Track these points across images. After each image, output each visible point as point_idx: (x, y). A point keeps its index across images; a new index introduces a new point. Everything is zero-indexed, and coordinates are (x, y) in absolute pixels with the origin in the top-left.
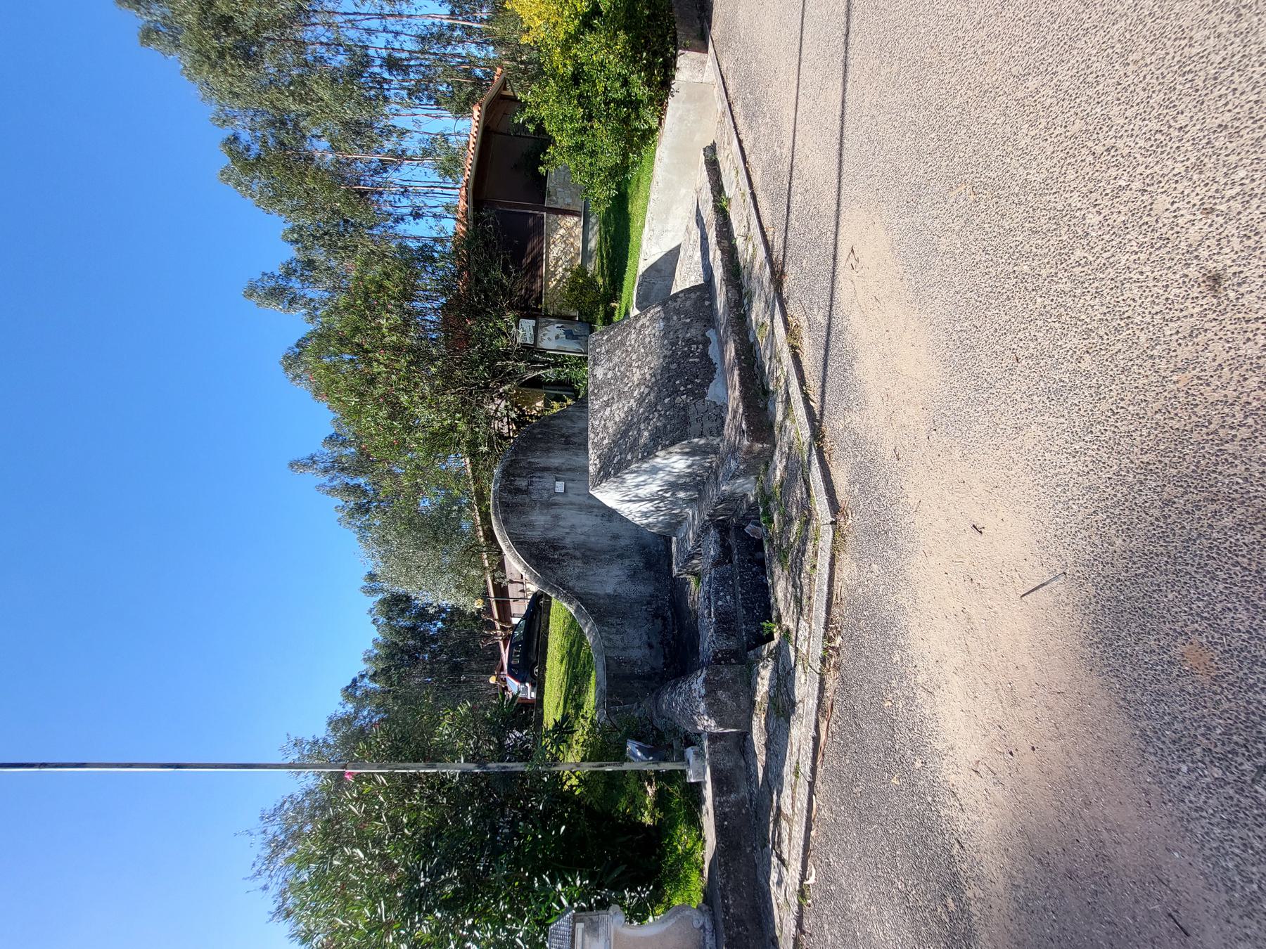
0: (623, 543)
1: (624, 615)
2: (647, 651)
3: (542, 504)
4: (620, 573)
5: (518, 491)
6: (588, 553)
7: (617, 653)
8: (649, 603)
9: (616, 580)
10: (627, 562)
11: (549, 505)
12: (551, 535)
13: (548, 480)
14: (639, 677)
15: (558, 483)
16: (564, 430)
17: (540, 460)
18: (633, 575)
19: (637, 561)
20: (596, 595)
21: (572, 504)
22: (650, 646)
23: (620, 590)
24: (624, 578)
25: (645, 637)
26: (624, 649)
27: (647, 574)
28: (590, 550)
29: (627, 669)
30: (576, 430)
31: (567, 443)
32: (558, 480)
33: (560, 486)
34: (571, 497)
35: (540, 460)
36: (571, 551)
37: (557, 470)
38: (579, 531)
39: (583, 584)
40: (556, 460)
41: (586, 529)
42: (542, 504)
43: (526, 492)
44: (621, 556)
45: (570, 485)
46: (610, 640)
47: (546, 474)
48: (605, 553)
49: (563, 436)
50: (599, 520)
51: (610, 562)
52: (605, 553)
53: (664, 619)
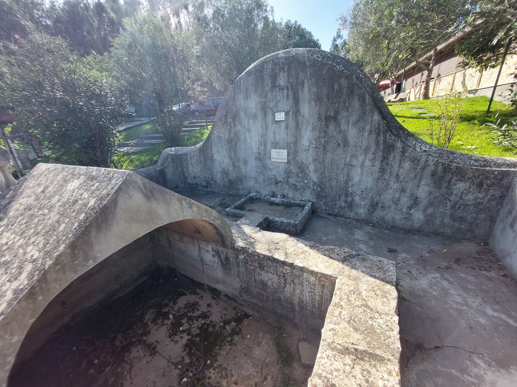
0: (242, 167)
1: (205, 165)
2: (193, 176)
3: (265, 102)
4: (225, 163)
5: (274, 78)
6: (233, 143)
7: (189, 159)
8: (212, 179)
9: (221, 161)
10: (231, 168)
11: (264, 109)
12: (242, 114)
13: (286, 104)
14: (183, 170)
15: (283, 114)
16: (344, 114)
17: (306, 94)
18: (225, 172)
19: (233, 175)
20: (212, 148)
21: (266, 128)
22: (195, 177)
23: (216, 163)
24: (223, 166)
25: (198, 175)
26: (191, 163)
27: (226, 180)
28: (236, 144)
29: (184, 165)
30: (344, 127)
31: (328, 119)
32: (287, 114)
33: (280, 116)
34: (272, 128)
35: (306, 94)
36: (233, 131)
37: (297, 112)
38: (247, 136)
39: (216, 140)
40: (308, 110)
41: (249, 140)
42: (265, 102)
43: (274, 86)
44: (234, 165)
45: (283, 125)
46: (194, 155)
47: (291, 101)
48: (235, 154)
49: (337, 113)
50: (255, 150)
51: (230, 158)
52: (235, 154)
53: (207, 187)
